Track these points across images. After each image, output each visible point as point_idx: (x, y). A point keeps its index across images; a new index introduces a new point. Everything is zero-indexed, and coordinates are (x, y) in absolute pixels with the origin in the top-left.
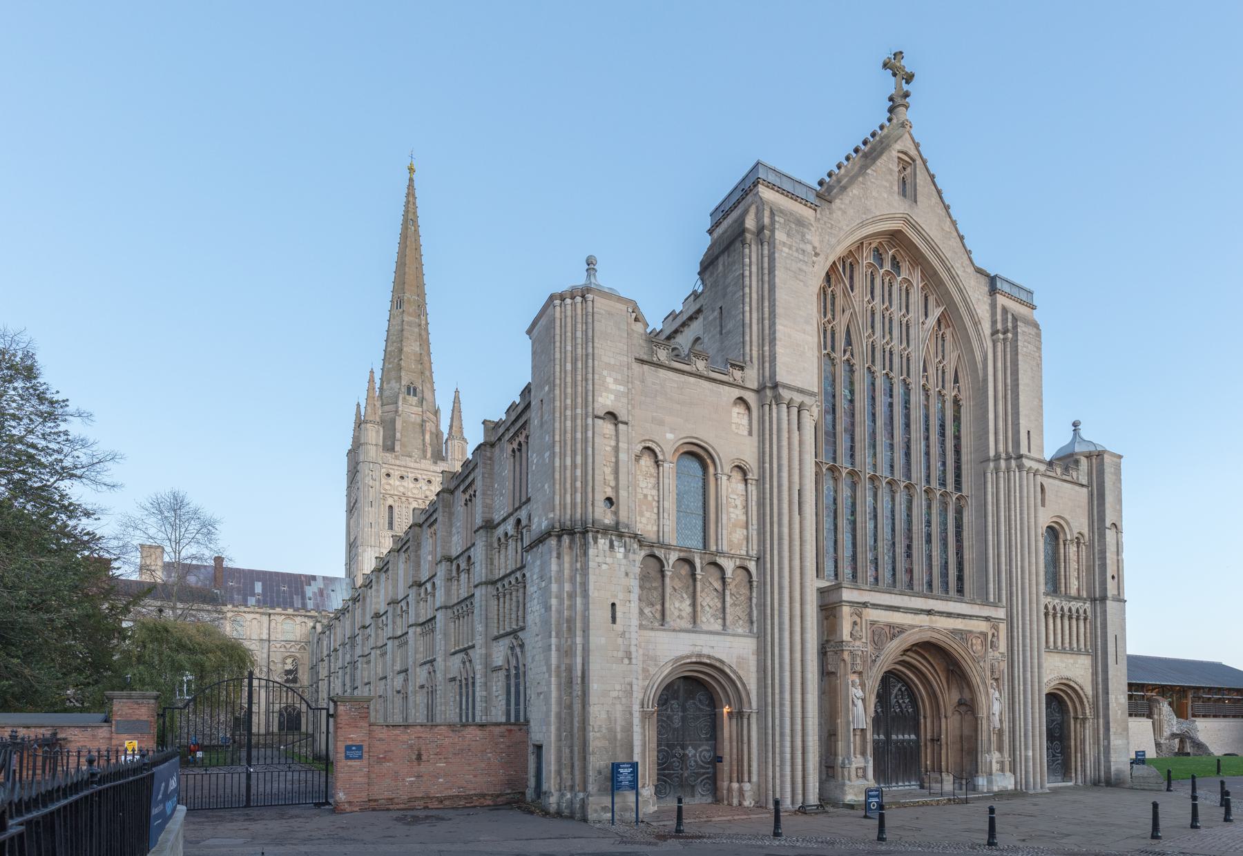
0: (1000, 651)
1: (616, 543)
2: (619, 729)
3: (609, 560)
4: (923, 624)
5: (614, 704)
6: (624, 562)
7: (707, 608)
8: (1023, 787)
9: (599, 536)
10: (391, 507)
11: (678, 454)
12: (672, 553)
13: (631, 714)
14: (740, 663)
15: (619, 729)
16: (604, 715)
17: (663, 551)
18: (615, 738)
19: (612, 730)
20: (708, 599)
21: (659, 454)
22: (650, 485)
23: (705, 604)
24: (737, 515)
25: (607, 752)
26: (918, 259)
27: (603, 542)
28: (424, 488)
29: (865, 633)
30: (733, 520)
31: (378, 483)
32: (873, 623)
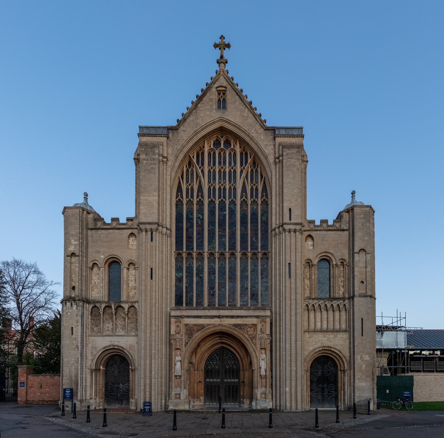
0: (267, 333)
2: (73, 376)
4: (216, 323)
5: (71, 366)
8: (284, 408)
11: (107, 264)
12: (103, 304)
13: (78, 370)
15: (73, 376)
16: (68, 371)
19: (71, 376)
21: (99, 265)
22: (97, 278)
24: (132, 284)
25: (69, 385)
29: (183, 330)
30: (130, 287)
32: (186, 325)
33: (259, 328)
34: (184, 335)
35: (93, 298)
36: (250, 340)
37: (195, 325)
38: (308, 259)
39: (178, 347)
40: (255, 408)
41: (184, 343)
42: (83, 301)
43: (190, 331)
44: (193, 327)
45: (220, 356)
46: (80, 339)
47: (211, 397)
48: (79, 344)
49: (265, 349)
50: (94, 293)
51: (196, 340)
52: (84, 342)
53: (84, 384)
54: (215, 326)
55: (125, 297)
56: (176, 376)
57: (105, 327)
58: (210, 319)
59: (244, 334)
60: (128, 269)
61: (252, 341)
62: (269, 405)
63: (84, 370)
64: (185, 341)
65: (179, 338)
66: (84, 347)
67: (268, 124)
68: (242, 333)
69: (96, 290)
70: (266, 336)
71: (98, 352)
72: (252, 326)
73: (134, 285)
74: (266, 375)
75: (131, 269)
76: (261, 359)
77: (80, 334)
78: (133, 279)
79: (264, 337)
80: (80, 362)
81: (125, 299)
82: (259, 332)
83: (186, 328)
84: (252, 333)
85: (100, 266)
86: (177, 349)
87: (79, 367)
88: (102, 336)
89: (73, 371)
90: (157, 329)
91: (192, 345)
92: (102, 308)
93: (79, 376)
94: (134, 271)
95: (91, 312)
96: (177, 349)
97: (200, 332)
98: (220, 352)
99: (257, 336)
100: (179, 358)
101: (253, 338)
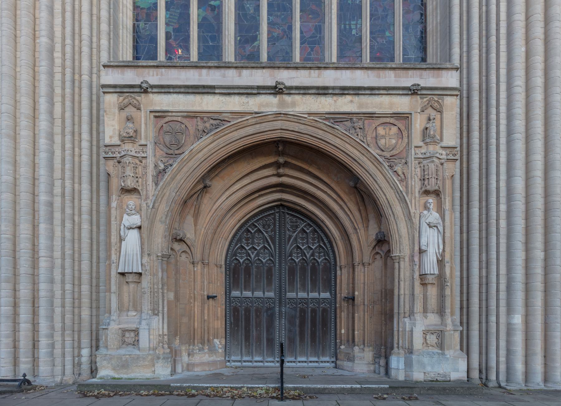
0: (444, 144)
4: (263, 110)
32: (159, 115)
33: (418, 126)
34: (150, 147)
36: (386, 164)
41: (151, 171)
44: (184, 121)
45: (274, 230)
47: (247, 338)
49: (437, 193)
51: (192, 164)
58: (244, 99)
61: (391, 167)
64: (156, 166)
65: (133, 153)
70: (441, 151)
79: (438, 155)
82: (417, 140)
83: (159, 125)
84: (394, 141)
91: (178, 177)
97: (206, 139)
98: (274, 219)
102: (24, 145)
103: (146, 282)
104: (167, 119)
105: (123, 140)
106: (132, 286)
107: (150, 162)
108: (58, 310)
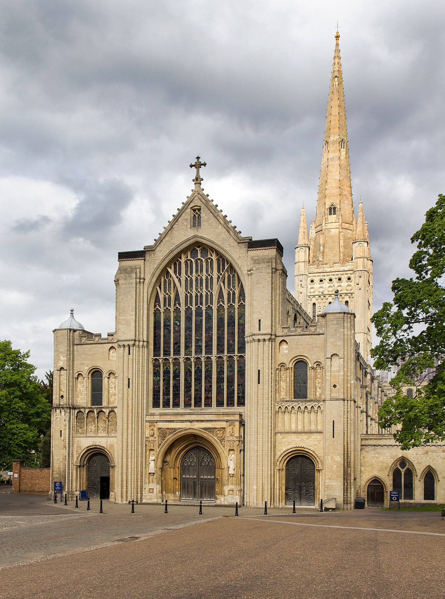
1: (62, 411)
3: (60, 417)
6: (64, 416)
7: (101, 428)
9: (57, 409)
10: (314, 304)
11: (91, 373)
12: (87, 409)
13: (66, 466)
14: (110, 447)
17: (83, 409)
18: (61, 474)
19: (60, 471)
20: (101, 424)
22: (82, 386)
23: (100, 426)
24: (112, 391)
26: (213, 250)
27: (58, 411)
28: (337, 285)
30: (111, 393)
31: (305, 289)
32: (159, 429)
34: (157, 437)
35: (78, 404)
36: (219, 442)
37: (168, 429)
38: (280, 364)
39: (152, 448)
40: (223, 504)
42: (70, 408)
43: (163, 434)
44: (166, 430)
46: (67, 440)
48: (67, 445)
50: (79, 399)
51: (168, 442)
52: (71, 442)
53: (70, 478)
54: (187, 429)
55: (106, 402)
56: (150, 473)
57: (88, 428)
59: (214, 437)
60: (109, 378)
61: (221, 442)
62: (236, 499)
63: (71, 466)
66: (71, 447)
67: (243, 235)
68: (212, 435)
69: (80, 397)
71: (83, 451)
72: (221, 429)
73: (114, 391)
74: (233, 474)
75: (111, 378)
76: (229, 460)
77: (67, 436)
78: (113, 386)
80: (67, 460)
81: (106, 405)
85: (84, 376)
86: (151, 450)
87: (67, 464)
88: (86, 437)
89: (62, 467)
90: (133, 432)
92: (86, 413)
93: (67, 471)
94: (114, 380)
95: (77, 416)
96: (151, 450)
99: (226, 438)
100: (153, 458)
101: (222, 440)
102: (125, 437)
103: (155, 476)
104: (161, 430)
105: (150, 436)
106: (152, 476)
107: (157, 442)
108: (133, 483)
